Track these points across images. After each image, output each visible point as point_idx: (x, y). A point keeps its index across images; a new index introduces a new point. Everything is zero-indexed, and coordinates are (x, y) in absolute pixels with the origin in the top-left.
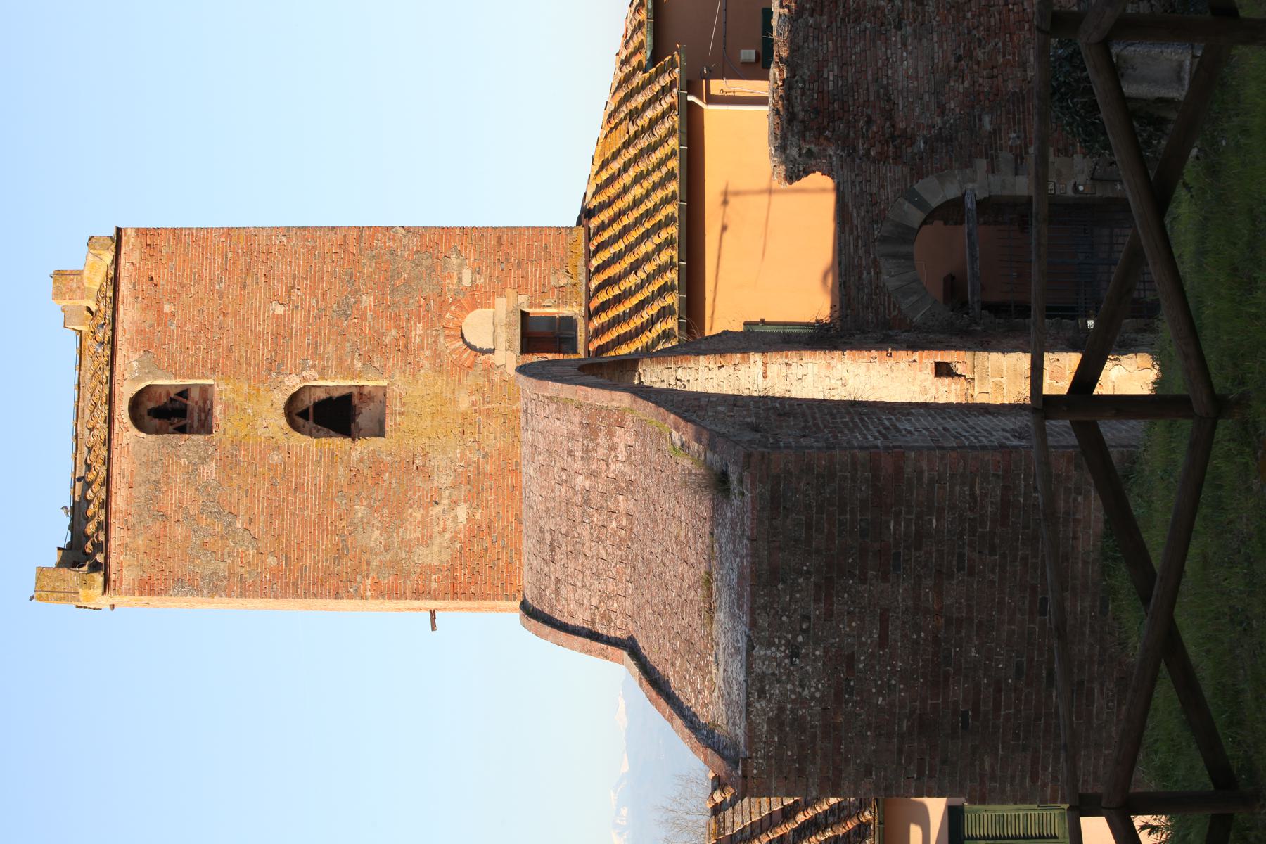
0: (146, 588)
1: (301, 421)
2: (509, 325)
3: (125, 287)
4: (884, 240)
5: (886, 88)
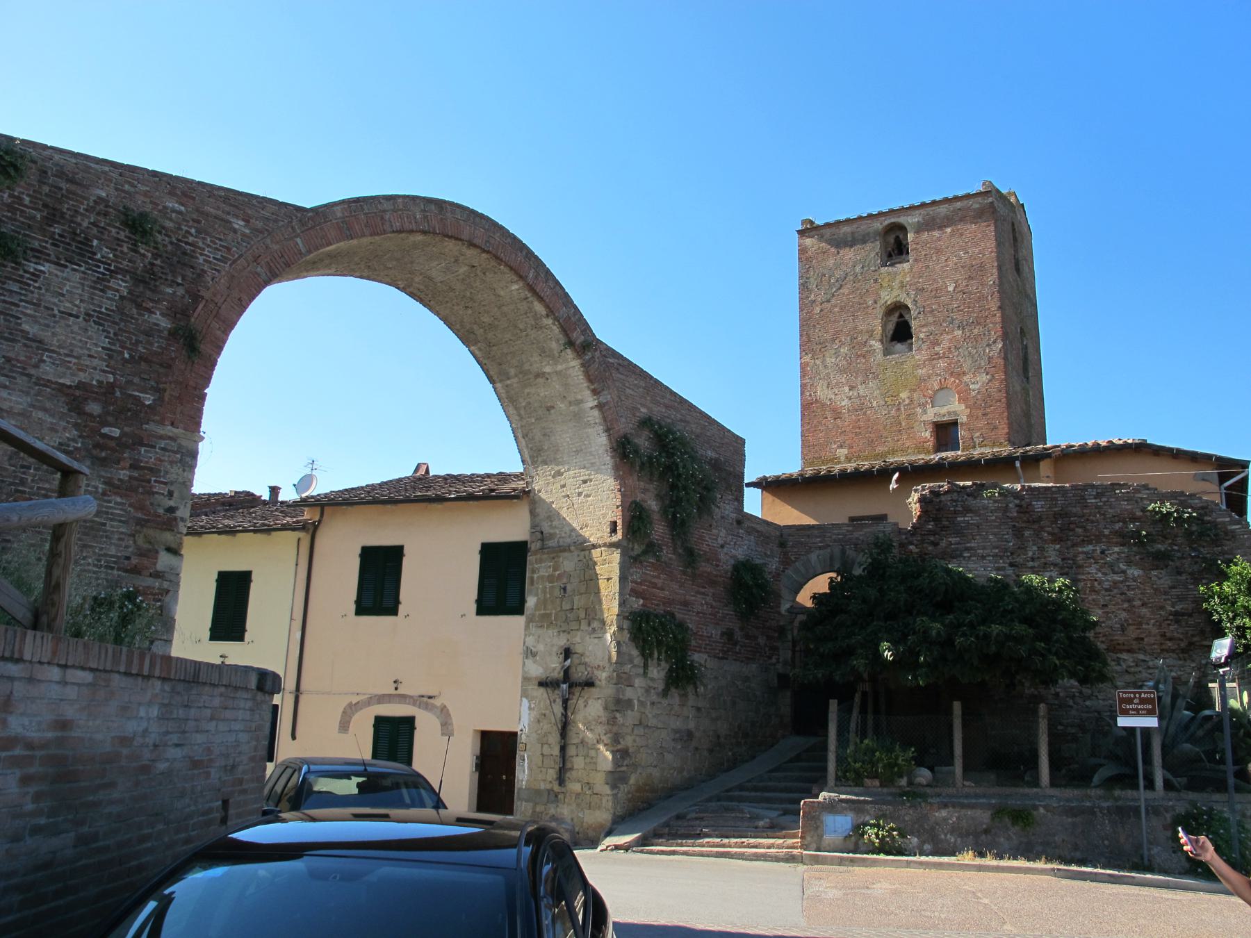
0: (802, 251)
1: (897, 315)
2: (949, 413)
3: (959, 204)
4: (843, 552)
5: (961, 556)
